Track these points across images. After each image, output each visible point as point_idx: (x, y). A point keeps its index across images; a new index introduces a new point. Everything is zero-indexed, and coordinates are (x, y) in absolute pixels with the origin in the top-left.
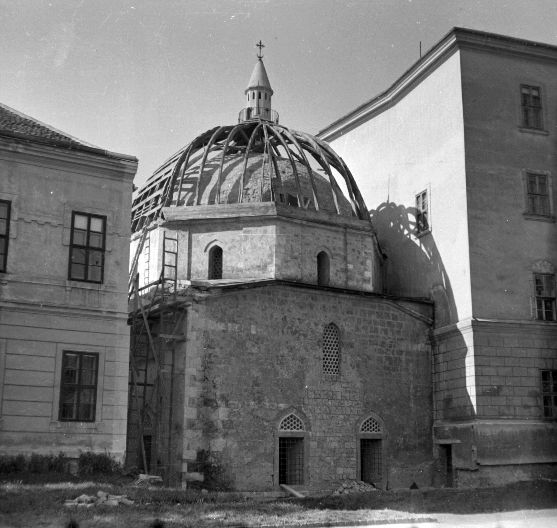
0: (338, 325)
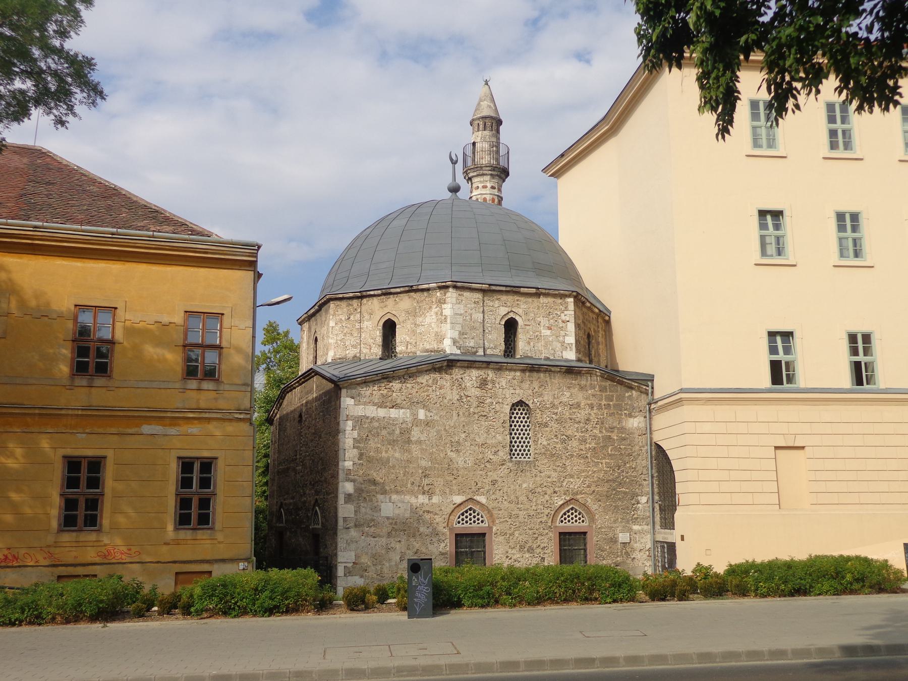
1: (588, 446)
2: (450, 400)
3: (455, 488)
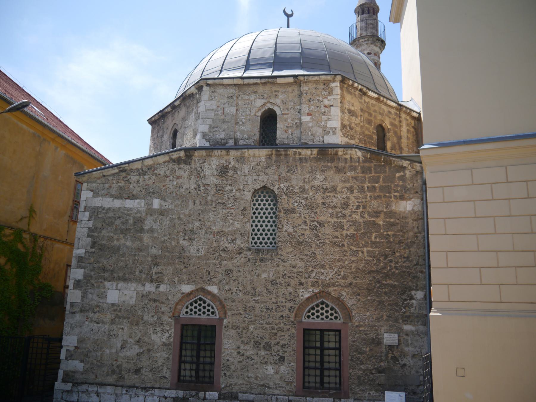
0: (272, 188)
1: (345, 232)
2: (187, 189)
3: (185, 277)
